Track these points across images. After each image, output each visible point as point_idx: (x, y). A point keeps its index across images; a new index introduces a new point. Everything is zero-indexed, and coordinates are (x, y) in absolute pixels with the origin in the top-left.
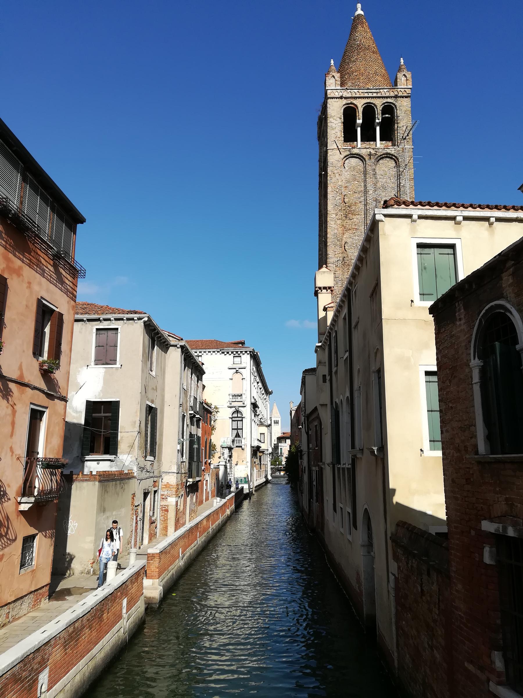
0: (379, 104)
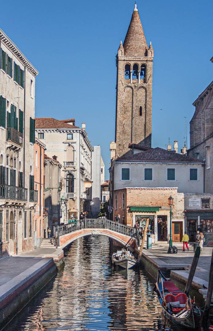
0: (140, 64)
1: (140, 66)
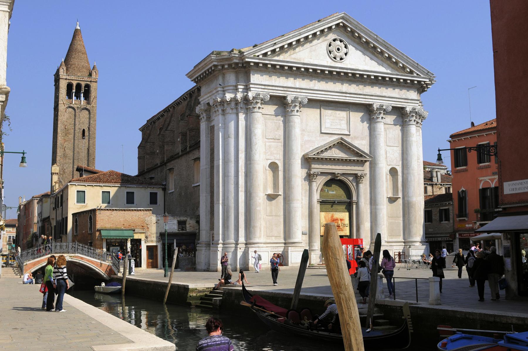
0: (83, 84)
1: (83, 86)
